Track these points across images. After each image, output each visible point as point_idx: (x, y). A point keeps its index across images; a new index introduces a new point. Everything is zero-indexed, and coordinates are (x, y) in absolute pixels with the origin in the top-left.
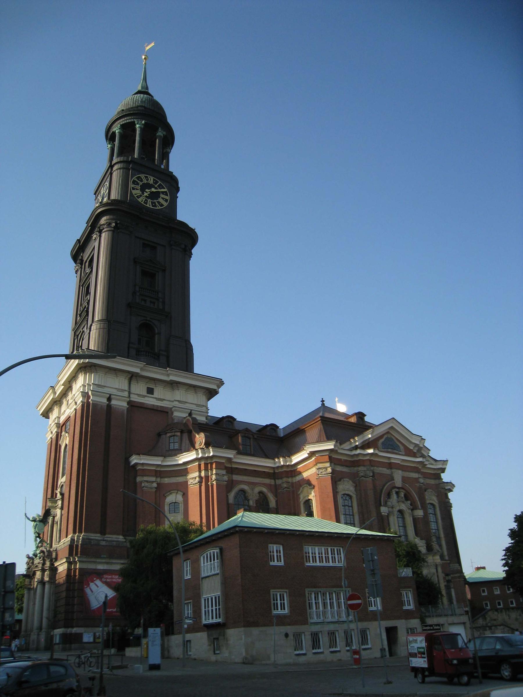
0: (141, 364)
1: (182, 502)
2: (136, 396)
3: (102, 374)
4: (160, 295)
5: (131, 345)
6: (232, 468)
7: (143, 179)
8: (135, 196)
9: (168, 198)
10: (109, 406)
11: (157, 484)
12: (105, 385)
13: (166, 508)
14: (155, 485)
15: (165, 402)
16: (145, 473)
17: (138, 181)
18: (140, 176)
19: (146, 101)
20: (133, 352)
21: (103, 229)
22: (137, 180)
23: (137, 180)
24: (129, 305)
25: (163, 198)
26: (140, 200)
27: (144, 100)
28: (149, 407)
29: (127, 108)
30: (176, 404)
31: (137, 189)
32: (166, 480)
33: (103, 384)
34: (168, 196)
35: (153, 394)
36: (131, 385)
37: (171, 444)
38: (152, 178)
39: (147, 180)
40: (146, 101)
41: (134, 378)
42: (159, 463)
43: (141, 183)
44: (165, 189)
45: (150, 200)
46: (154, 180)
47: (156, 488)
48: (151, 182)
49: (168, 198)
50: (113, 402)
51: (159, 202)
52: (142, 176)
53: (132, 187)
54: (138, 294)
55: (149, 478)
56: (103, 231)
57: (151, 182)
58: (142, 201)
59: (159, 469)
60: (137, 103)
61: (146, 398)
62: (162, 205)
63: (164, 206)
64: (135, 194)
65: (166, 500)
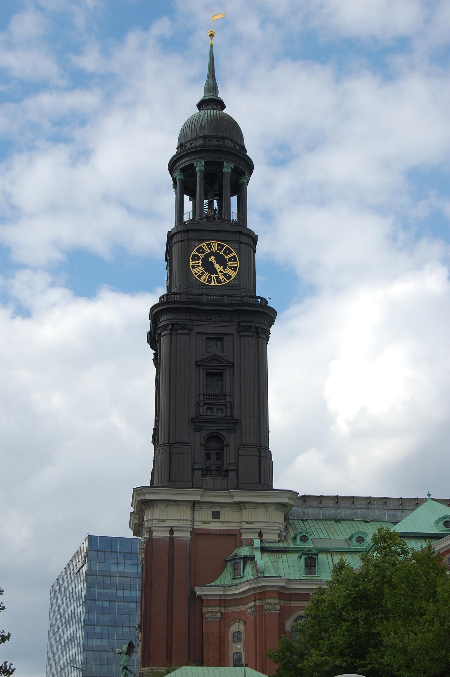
0: (201, 491)
1: (244, 631)
2: (200, 524)
3: (163, 507)
4: (228, 398)
5: (196, 467)
6: (290, 593)
7: (205, 249)
8: (196, 276)
9: (237, 264)
10: (172, 540)
11: (222, 614)
12: (166, 518)
13: (231, 637)
14: (219, 615)
15: (232, 524)
16: (211, 602)
17: (199, 254)
18: (200, 246)
19: (206, 126)
20: (198, 474)
21: (161, 333)
22: (197, 254)
23: (197, 254)
24: (193, 421)
25: (230, 267)
26: (202, 280)
27: (203, 124)
28: (215, 533)
29: (186, 140)
30: (244, 525)
31: (198, 266)
32: (230, 609)
33: (164, 518)
34: (237, 261)
35: (219, 518)
36: (195, 512)
37: (235, 570)
38: (216, 243)
39: (210, 249)
40: (206, 126)
41: (196, 505)
42: (221, 593)
43: (202, 256)
44: (233, 252)
46: (219, 245)
47: (220, 618)
48: (215, 249)
49: (237, 264)
50: (176, 535)
52: (204, 245)
53: (192, 265)
54: (202, 404)
55: (213, 609)
56: (161, 335)
57: (215, 249)
58: (204, 281)
59: (223, 598)
60: (195, 131)
61: (212, 524)
63: (232, 277)
64: (196, 274)
65: (230, 630)
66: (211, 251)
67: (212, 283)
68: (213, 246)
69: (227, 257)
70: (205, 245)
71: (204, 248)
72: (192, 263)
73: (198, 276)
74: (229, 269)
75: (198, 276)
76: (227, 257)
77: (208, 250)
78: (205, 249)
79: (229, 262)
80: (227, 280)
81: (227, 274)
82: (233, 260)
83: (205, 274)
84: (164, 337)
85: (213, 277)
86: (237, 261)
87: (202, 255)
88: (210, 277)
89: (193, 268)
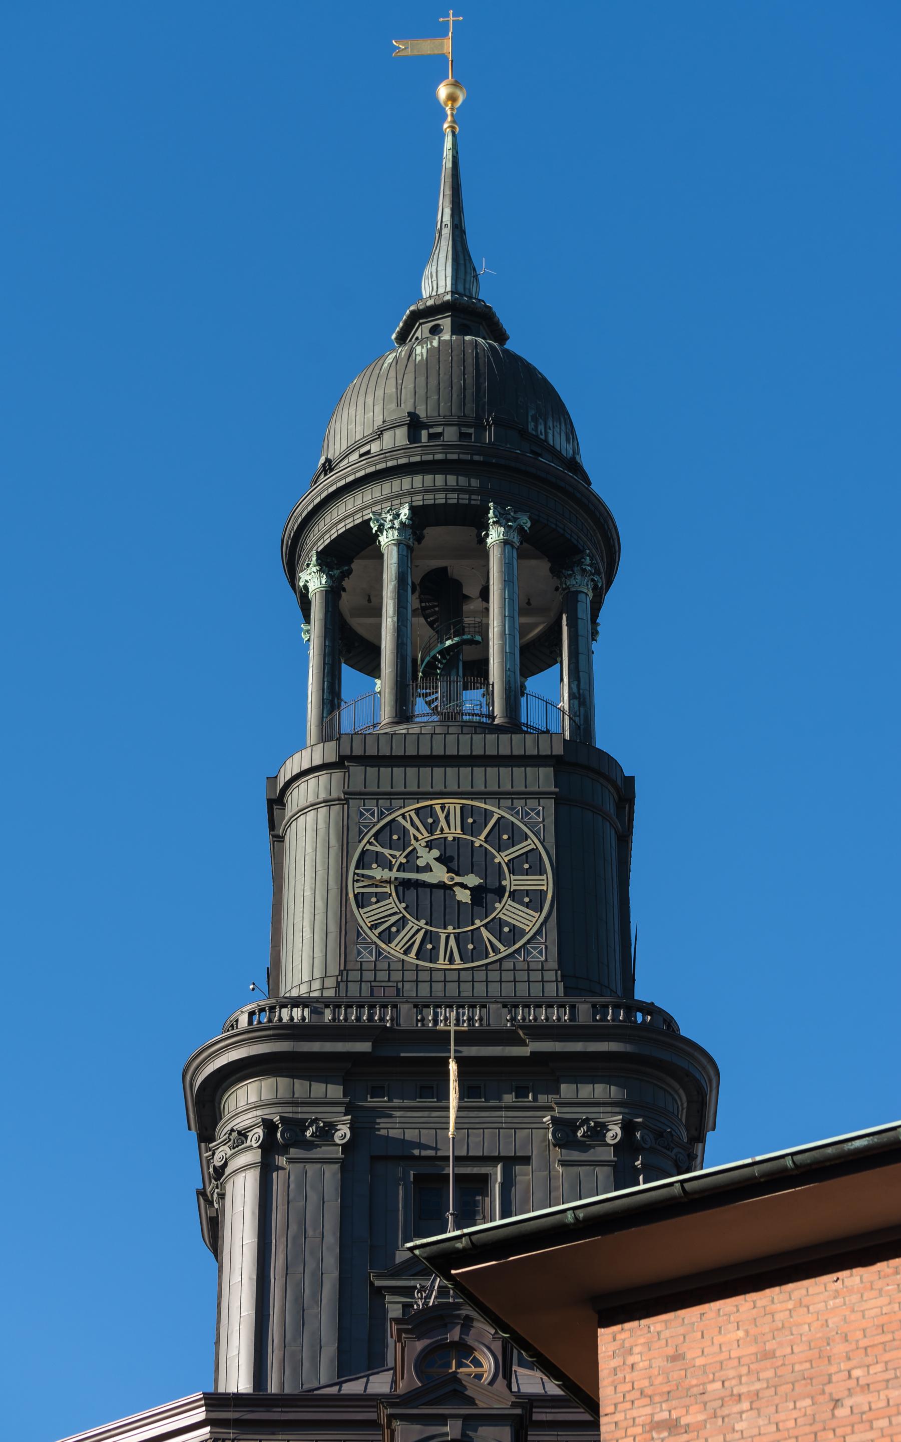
7: (412, 831)
8: (373, 936)
9: (545, 883)
38: (454, 805)
45: (450, 929)
51: (496, 927)
56: (228, 1171)
57: (453, 831)
62: (516, 933)
63: (523, 933)
66: (437, 835)
67: (441, 961)
68: (442, 816)
69: (502, 858)
70: (413, 814)
71: (408, 826)
72: (356, 885)
73: (380, 936)
74: (510, 902)
75: (380, 936)
76: (502, 858)
77: (426, 834)
78: (412, 831)
79: (513, 877)
80: (502, 948)
81: (501, 923)
82: (526, 866)
83: (410, 924)
84: (239, 1178)
85: (443, 937)
86: (542, 871)
87: (397, 854)
88: (430, 937)
89: (360, 905)
